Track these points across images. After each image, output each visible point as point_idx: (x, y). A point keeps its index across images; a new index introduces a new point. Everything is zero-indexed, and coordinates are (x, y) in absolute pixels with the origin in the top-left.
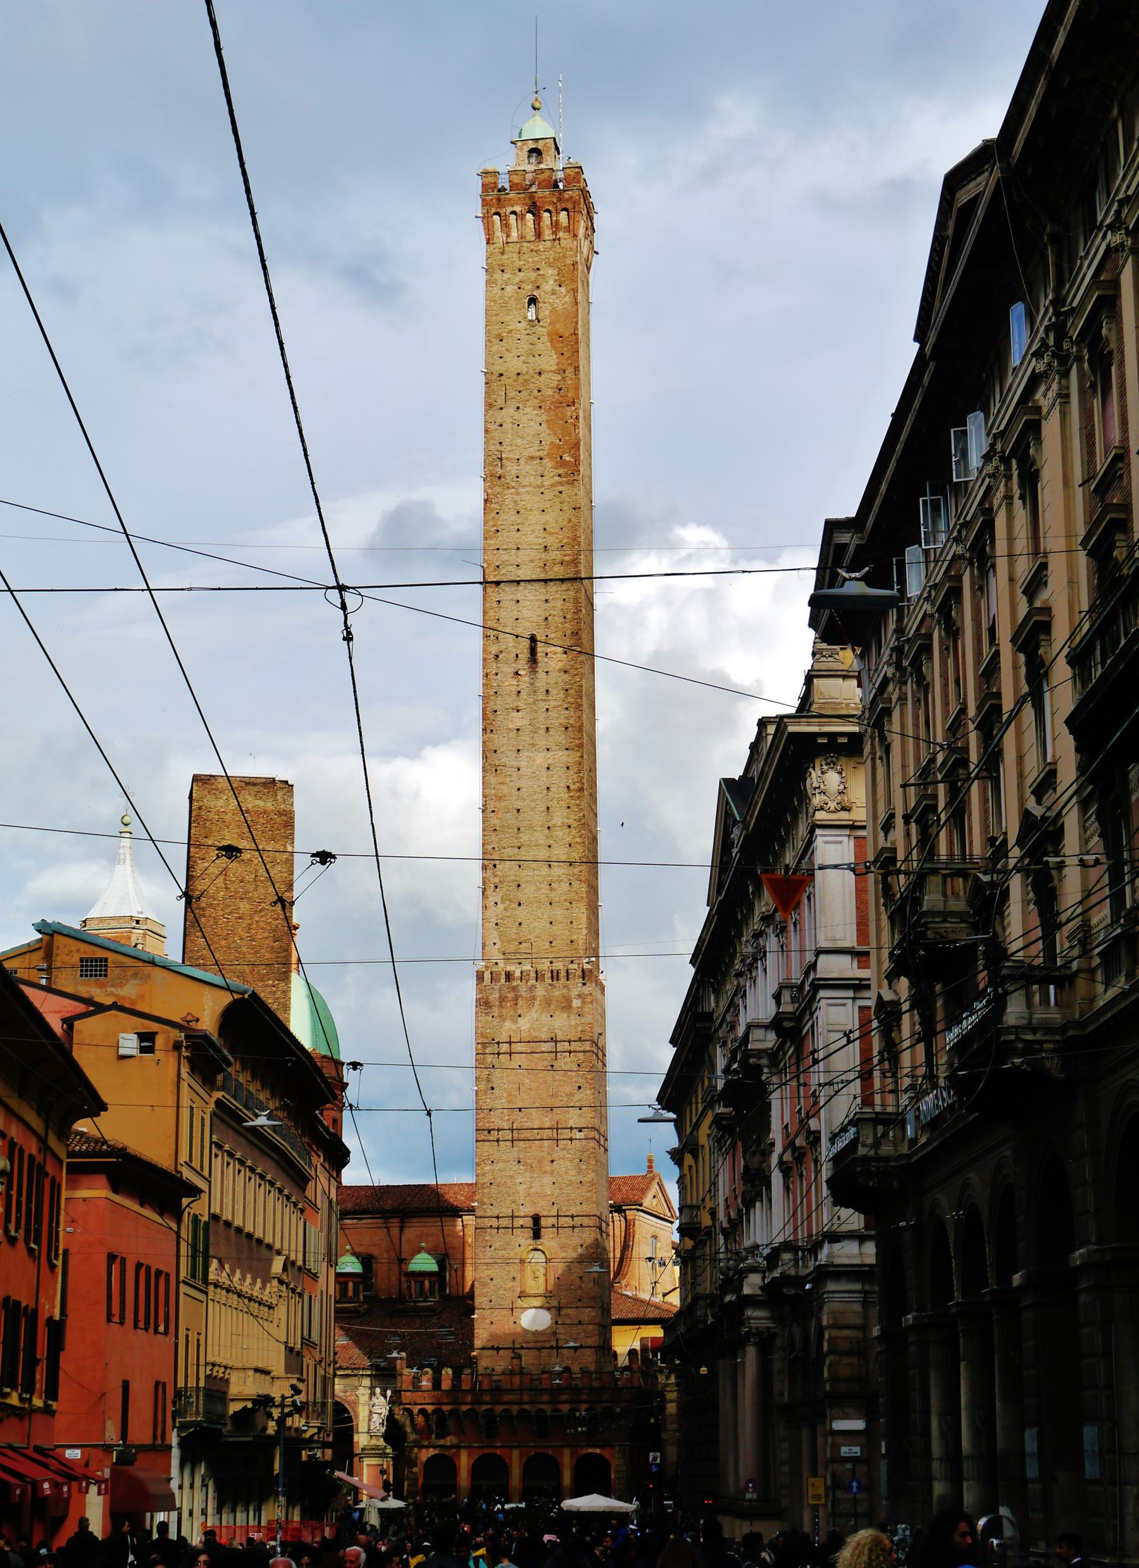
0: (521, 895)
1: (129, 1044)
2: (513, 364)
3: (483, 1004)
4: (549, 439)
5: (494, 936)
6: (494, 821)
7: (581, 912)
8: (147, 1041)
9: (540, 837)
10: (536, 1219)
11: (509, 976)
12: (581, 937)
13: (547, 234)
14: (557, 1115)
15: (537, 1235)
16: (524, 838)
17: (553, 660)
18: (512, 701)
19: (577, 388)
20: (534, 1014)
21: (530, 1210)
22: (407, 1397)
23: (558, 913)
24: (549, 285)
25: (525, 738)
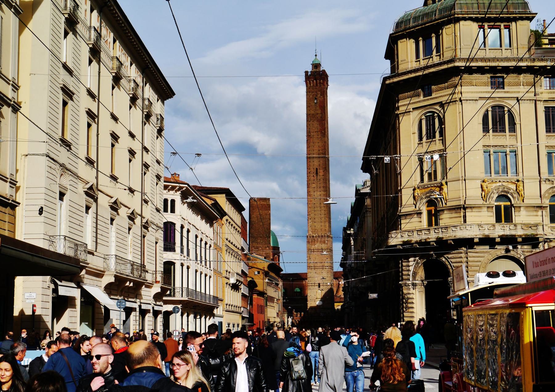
0: (315, 221)
1: (256, 273)
2: (312, 112)
3: (308, 242)
4: (319, 128)
5: (310, 229)
6: (310, 206)
7: (327, 224)
8: (259, 273)
9: (319, 209)
10: (319, 284)
11: (313, 237)
12: (327, 228)
13: (319, 85)
14: (323, 264)
15: (319, 287)
16: (316, 209)
17: (321, 173)
18: (313, 182)
19: (325, 117)
20: (318, 244)
21: (318, 282)
22: (295, 318)
23: (323, 224)
24: (319, 95)
25: (316, 189)
